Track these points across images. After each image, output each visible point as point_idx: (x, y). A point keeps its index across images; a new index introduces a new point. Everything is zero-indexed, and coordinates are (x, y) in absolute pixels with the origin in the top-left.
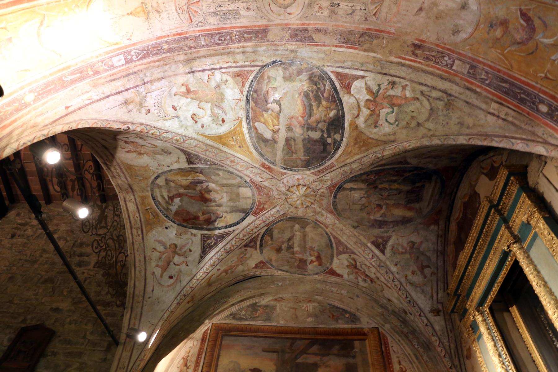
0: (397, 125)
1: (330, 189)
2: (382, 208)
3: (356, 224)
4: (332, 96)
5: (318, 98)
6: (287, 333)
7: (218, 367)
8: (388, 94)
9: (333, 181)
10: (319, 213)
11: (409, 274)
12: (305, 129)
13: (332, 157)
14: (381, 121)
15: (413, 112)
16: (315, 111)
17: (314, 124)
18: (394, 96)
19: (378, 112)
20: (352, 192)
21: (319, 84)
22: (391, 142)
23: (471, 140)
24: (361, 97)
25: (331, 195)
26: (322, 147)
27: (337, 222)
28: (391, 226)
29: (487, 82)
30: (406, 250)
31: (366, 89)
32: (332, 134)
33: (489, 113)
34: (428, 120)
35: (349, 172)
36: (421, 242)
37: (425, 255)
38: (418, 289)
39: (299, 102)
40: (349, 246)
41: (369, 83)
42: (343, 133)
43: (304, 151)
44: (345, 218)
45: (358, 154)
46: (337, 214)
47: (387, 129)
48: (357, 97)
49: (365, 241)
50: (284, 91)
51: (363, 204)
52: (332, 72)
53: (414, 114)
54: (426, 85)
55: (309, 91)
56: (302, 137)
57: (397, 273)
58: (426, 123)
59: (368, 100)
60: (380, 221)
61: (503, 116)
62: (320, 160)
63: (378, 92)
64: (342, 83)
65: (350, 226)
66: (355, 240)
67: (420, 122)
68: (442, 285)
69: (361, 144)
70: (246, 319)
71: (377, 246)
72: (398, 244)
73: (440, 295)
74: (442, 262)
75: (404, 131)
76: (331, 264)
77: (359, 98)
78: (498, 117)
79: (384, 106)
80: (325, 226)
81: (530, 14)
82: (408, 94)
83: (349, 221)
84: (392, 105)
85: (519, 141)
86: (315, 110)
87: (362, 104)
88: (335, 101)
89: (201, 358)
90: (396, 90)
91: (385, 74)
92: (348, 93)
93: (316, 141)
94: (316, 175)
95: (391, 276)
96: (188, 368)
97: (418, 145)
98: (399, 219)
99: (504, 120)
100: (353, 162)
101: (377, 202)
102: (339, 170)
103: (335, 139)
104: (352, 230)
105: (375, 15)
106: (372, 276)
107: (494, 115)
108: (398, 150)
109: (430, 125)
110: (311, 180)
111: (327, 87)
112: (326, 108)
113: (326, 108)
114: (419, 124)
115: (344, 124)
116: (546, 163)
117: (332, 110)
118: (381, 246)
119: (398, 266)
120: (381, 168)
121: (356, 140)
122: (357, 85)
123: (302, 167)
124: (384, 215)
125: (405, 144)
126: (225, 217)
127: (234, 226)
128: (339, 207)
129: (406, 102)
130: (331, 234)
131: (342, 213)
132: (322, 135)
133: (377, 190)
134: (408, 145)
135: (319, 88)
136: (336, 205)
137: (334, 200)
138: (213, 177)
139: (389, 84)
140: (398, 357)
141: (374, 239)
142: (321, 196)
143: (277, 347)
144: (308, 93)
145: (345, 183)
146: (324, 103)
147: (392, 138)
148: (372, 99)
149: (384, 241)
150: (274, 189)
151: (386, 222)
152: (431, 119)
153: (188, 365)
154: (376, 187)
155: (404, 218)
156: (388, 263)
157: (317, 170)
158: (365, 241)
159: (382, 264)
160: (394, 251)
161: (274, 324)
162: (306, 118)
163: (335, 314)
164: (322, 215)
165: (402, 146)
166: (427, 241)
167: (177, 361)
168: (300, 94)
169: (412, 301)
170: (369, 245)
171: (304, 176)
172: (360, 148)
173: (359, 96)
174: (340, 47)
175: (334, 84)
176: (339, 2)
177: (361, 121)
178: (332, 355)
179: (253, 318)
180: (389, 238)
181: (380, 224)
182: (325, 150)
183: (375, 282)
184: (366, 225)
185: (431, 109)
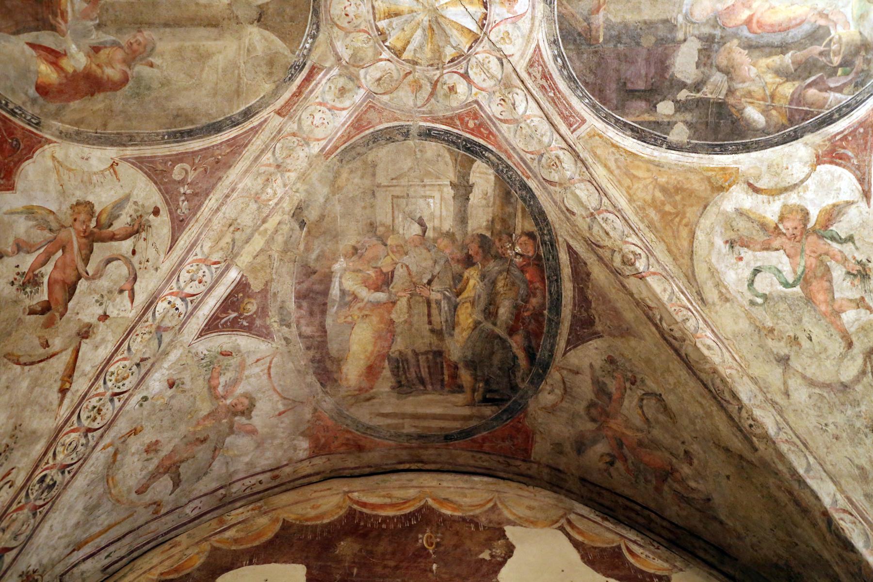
0: (752, 303)
1: (473, 111)
2: (378, 289)
3: (312, 215)
4: (807, 113)
5: (804, 70)
8: (832, 264)
9: (504, 127)
10: (353, 78)
11: (147, 437)
12: (706, 30)
13: (606, 119)
14: (752, 257)
15: (810, 339)
16: (764, 62)
17: (721, 59)
18: (830, 281)
19: (776, 243)
20: (449, 192)
21: (846, 74)
22: (699, 293)
23: (847, 517)
24: (809, 195)
25: (435, 120)
26: (641, 85)
27: (315, 148)
28: (308, 330)
30: (224, 397)
31: (834, 206)
32: (688, 117)
34: (812, 383)
35: (555, 177)
36: (253, 432)
37: (213, 458)
38: (100, 490)
39: (799, 11)
40: (211, 203)
41: (853, 211)
42: (694, 149)
43: (626, 26)
44: (337, 175)
45: (631, 200)
46: (353, 147)
47: (734, 276)
48: (809, 182)
49: (245, 258)
51: (392, 230)
53: (805, 343)
55: (828, 44)
56: (680, 19)
57: (145, 399)
58: (799, 381)
59: (806, 214)
60: (326, 293)
62: (591, 79)
63: (833, 239)
64: (845, 138)
65: (301, 196)
66: (246, 220)
67: (794, 363)
68: (123, 552)
69: (668, 208)
71: (230, 303)
72: (242, 366)
73: (88, 565)
74: (196, 512)
75: (744, 325)
76: (65, 136)
77: (807, 188)
79: (798, 258)
80: (288, 104)
82: (849, 317)
83: (323, 191)
84: (804, 280)
86: (769, 61)
87: (793, 199)
88: (791, 122)
90: (847, 283)
92: (817, 157)
93: (662, 64)
94: (531, 64)
95: (129, 384)
97: (724, 371)
98: (333, 347)
100: (599, 189)
101: (400, 272)
102: (557, 142)
103: (670, 125)
104: (287, 206)
106: (84, 307)
108: (679, 318)
109: (801, 394)
110: (508, 49)
111: (832, 96)
112: (772, 97)
113: (772, 97)
114: (784, 361)
115: (723, 150)
117: (765, 112)
118: (235, 313)
119: (170, 392)
120: (566, 271)
121: (678, 189)
123: (561, 17)
124: (349, 299)
125: (709, 333)
128: (383, 153)
129: (824, 314)
130: (255, 130)
131: (358, 163)
132: (684, 85)
133: (457, 268)
134: (709, 342)
135: (833, 72)
136: (391, 140)
137: (414, 131)
139: (859, 263)
141: (256, 285)
142: (435, 85)
144: (823, 38)
145: (493, 165)
146: (788, 89)
147: (711, 294)
148: (809, 226)
149: (251, 320)
151: (324, 312)
152: (817, 391)
154: (468, 261)
155: (339, 362)
156: (174, 356)
157: (553, 68)
158: (245, 258)
159: (167, 337)
160: (213, 365)
162: (745, 32)
164: (343, 91)
165: (697, 329)
166: (259, 445)
169: (54, 493)
170: (233, 275)
171: (525, 24)
172: (653, 204)
173: (812, 187)
175: (841, 116)
177: (738, 199)
180: (265, 334)
181: (314, 295)
182: (629, 93)
183: (49, 324)
184: (308, 249)
185: (845, 386)
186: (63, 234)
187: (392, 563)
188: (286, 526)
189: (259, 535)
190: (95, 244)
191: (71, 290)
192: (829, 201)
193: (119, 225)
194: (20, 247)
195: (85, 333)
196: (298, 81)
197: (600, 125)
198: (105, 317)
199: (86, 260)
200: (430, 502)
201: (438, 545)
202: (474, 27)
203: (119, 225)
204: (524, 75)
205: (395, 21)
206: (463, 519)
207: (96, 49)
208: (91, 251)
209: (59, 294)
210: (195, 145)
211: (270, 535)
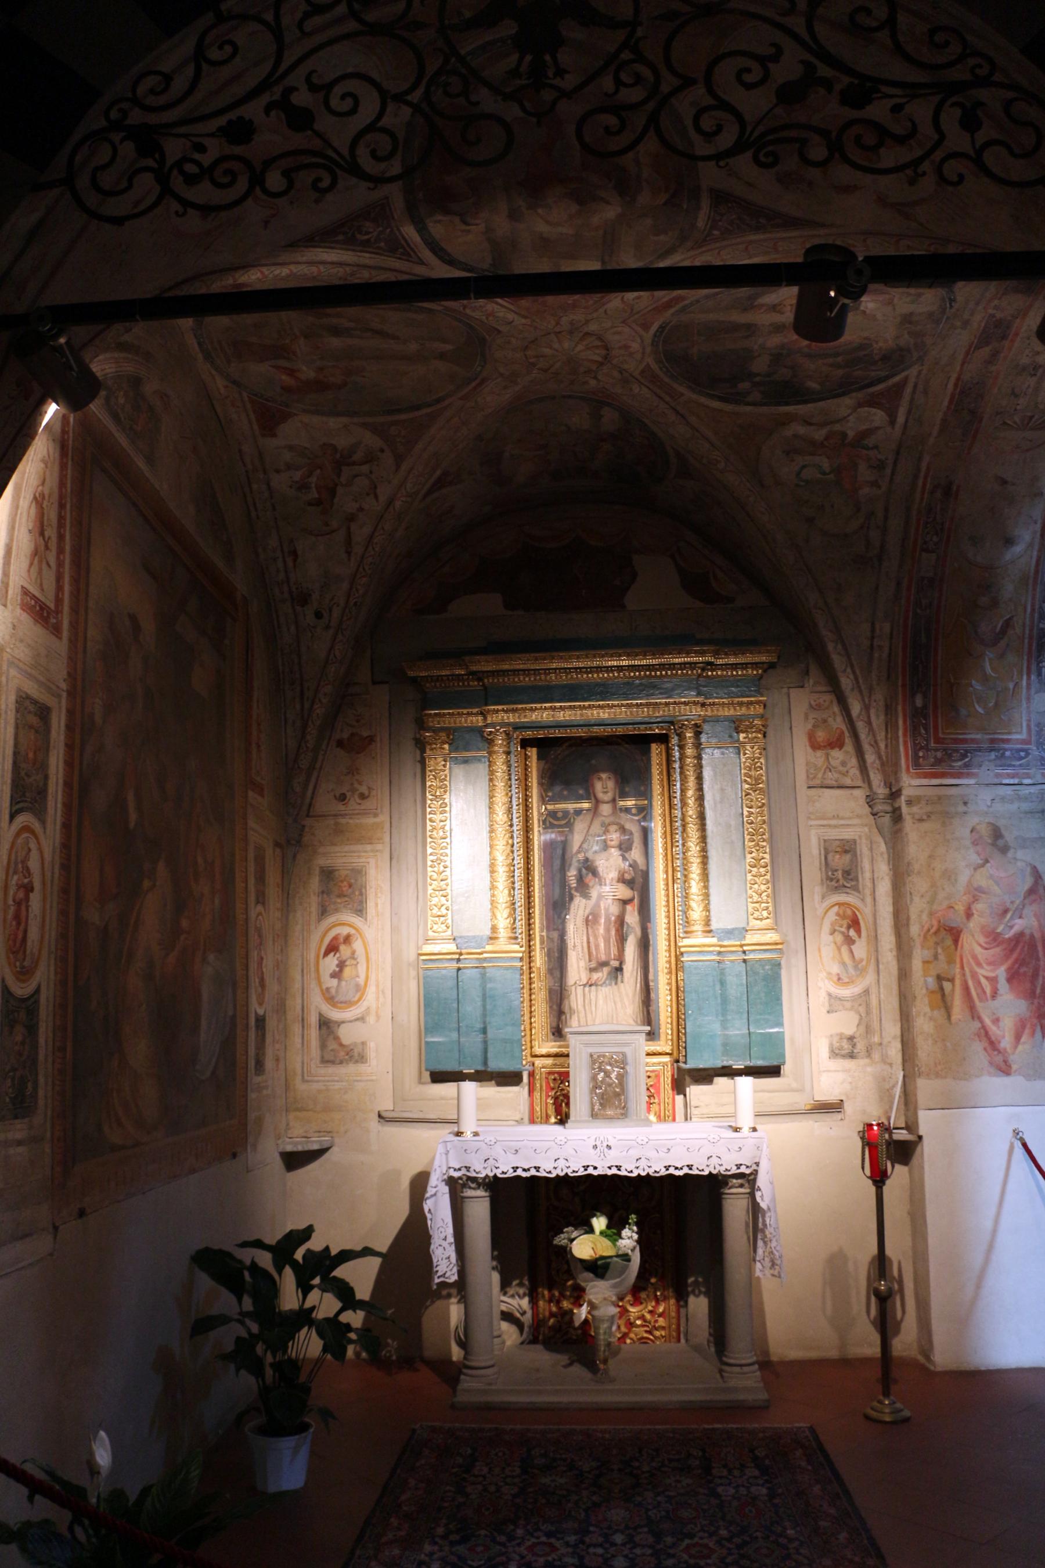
0: (797, 485)
15: (832, 506)
29: (919, 611)
31: (868, 430)
33: (873, 624)
42: (765, 404)
48: (851, 417)
50: (879, 316)
52: (906, 379)
54: (886, 518)
59: (844, 435)
61: (875, 644)
78: (873, 638)
81: (1010, 632)
85: (852, 676)
91: (898, 453)
94: (643, 372)
99: (872, 647)
105: (1005, 423)
107: (873, 630)
110: (626, 366)
111: (873, 374)
115: (787, 404)
116: (802, 687)
122: (878, 417)
126: (469, 231)
127: (441, 258)
138: (649, 221)
139: (879, 460)
150: (595, 315)
164: (505, 388)
168: (866, 338)
170: (438, 473)
174: (956, 385)
176: (1039, 374)
191: (333, 492)
192: (864, 427)
193: (358, 456)
194: (289, 467)
195: (351, 518)
196: (473, 384)
197: (694, 396)
198: (361, 509)
199: (339, 476)
202: (600, 344)
203: (358, 456)
204: (639, 377)
205: (541, 359)
207: (321, 369)
210: (403, 417)
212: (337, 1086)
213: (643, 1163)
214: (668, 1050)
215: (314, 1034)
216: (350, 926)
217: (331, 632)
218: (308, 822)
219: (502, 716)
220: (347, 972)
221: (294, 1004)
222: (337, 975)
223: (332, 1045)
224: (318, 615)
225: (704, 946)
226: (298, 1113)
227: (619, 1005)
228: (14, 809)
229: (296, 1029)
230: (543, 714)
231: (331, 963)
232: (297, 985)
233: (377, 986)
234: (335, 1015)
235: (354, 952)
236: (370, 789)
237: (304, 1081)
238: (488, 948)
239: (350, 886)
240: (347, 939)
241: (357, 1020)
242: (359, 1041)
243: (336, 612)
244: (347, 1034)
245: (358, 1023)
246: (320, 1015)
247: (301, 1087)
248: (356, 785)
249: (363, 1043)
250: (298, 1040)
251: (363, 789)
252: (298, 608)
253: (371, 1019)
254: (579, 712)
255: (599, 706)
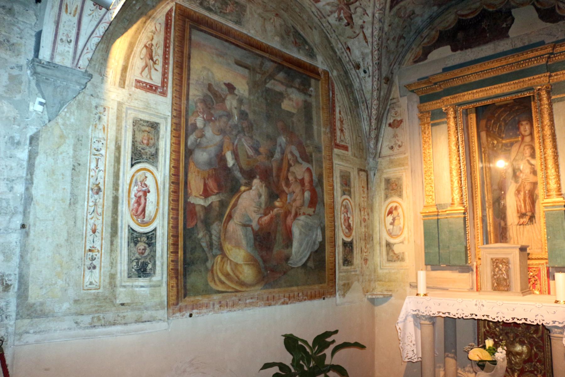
6: (257, 48)
7: (191, 72)
70: (216, 13)
72: (405, 8)
89: (169, 52)
96: (155, 63)
106: (357, 21)
140: (340, 107)
143: (249, 62)
153: (155, 59)
159: (382, 20)
161: (245, 32)
163: (297, 41)
167: (139, 49)
178: (294, 87)
179: (223, 14)
183: (352, 27)
186: (340, 6)
187: (475, 37)
188: (441, 32)
189: (434, 38)
190: (350, 6)
191: (351, 18)
195: (362, 27)
198: (364, 22)
199: (350, 10)
200: (485, 7)
201: (489, 25)
206: (497, 11)
208: (350, 8)
209: (349, 20)
211: (437, 37)
212: (393, 271)
213: (500, 315)
214: (546, 256)
215: (384, 249)
216: (397, 202)
217: (371, 77)
218: (380, 160)
219: (450, 100)
220: (396, 222)
221: (376, 237)
222: (392, 224)
223: (391, 254)
224: (365, 72)
225: (555, 202)
226: (379, 282)
227: (535, 235)
228: (133, 163)
229: (377, 247)
230: (468, 96)
231: (390, 219)
232: (377, 229)
233: (408, 228)
234: (392, 241)
235: (398, 214)
236: (402, 142)
237: (381, 269)
238: (449, 208)
239: (396, 185)
240: (396, 208)
241: (400, 243)
242: (401, 252)
243: (370, 68)
244: (397, 249)
245: (401, 244)
246: (386, 241)
247: (380, 271)
248: (397, 142)
249: (403, 253)
250: (378, 252)
251: (400, 143)
252: (357, 71)
253: (406, 242)
254: (485, 93)
255: (495, 88)
